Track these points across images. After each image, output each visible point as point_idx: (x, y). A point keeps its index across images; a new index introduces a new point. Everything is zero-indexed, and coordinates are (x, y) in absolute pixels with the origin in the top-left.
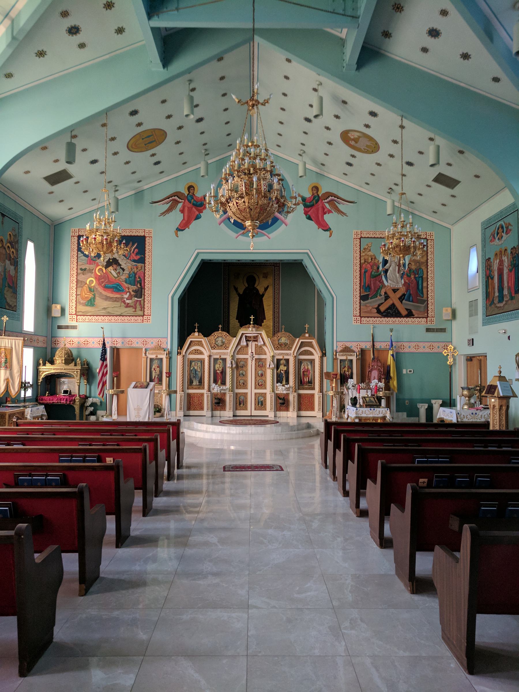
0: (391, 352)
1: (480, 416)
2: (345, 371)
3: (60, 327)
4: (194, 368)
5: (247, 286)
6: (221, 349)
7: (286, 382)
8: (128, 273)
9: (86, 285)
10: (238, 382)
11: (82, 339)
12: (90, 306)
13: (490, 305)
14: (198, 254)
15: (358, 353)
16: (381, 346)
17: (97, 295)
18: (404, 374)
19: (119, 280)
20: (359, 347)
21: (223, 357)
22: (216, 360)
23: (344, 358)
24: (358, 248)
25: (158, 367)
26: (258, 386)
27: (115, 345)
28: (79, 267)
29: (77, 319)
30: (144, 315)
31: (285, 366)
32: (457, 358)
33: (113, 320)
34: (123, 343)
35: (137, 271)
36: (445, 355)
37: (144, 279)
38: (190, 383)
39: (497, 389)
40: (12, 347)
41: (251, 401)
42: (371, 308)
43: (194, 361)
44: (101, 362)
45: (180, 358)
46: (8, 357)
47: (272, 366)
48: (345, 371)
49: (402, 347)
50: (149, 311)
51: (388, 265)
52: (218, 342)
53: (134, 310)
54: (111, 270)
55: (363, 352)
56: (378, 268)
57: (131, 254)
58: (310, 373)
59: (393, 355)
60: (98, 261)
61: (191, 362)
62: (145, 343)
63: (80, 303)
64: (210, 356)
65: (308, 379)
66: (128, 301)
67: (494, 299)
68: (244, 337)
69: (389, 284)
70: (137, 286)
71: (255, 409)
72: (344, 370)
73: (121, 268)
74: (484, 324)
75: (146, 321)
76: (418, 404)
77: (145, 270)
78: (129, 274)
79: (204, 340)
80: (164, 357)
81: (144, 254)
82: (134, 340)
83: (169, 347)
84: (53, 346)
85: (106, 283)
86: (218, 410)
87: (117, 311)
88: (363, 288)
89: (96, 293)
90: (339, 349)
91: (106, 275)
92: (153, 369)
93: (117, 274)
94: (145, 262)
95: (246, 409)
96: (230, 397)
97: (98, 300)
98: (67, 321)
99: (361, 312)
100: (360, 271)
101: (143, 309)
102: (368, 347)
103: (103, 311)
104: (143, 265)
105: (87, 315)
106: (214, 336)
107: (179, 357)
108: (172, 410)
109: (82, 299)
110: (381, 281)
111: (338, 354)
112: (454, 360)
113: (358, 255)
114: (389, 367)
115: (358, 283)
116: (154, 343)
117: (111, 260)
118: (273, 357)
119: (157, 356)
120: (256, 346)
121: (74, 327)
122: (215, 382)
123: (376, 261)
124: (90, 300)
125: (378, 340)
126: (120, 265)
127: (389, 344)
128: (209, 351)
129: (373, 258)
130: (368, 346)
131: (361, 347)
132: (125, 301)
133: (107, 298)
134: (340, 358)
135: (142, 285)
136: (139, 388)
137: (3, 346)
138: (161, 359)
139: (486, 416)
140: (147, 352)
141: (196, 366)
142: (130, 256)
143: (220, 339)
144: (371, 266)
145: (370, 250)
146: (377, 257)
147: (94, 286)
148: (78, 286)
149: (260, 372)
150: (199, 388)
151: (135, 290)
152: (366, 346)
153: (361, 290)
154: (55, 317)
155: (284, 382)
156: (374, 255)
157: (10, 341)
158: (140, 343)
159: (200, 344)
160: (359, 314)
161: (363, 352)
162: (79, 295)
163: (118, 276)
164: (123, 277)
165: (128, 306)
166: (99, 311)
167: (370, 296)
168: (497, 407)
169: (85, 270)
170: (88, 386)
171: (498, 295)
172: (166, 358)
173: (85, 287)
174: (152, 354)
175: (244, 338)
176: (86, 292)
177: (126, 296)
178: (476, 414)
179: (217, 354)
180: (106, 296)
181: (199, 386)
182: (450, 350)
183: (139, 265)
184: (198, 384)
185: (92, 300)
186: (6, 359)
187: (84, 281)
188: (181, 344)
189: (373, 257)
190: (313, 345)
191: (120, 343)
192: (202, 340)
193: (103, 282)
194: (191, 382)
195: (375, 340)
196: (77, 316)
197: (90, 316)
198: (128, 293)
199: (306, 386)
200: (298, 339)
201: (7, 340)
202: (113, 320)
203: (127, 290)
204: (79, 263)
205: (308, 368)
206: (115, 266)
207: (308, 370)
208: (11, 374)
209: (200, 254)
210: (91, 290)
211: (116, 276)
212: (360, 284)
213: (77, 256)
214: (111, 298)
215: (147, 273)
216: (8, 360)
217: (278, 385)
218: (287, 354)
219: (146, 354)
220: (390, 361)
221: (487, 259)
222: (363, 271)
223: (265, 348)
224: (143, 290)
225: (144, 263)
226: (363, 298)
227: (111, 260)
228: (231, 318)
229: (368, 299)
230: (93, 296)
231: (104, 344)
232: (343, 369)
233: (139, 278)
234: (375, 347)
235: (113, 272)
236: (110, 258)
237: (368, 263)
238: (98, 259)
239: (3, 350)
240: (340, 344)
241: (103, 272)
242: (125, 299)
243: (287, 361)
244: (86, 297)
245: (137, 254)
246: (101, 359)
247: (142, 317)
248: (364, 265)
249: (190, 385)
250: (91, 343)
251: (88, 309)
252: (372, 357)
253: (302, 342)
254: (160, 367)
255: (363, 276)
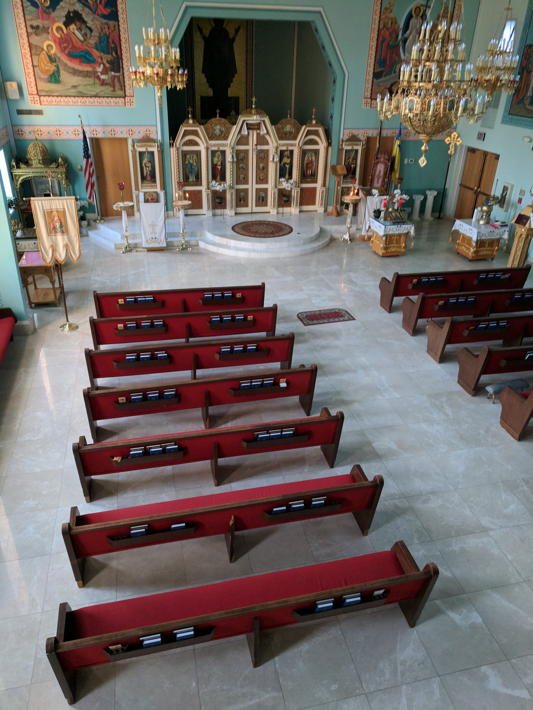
0: (398, 142)
1: (496, 233)
2: (349, 162)
3: (20, 112)
4: (189, 162)
5: (214, 25)
6: (219, 139)
7: (289, 176)
8: (98, 35)
9: (44, 52)
10: (238, 177)
11: (52, 128)
12: (55, 83)
13: (518, 103)
14: (187, 8)
15: (364, 143)
16: (387, 134)
17: (60, 67)
18: (406, 164)
19: (86, 45)
20: (365, 135)
21: (222, 148)
22: (214, 153)
23: (349, 148)
24: (379, 8)
25: (150, 162)
26: (259, 180)
27: (95, 136)
28: (29, 23)
29: (40, 102)
30: (125, 97)
31: (288, 158)
32: (459, 148)
33: (87, 102)
34: (104, 133)
35: (110, 33)
36: (448, 143)
37: (120, 45)
38: (186, 179)
39: (529, 220)
40: (64, 209)
41: (252, 198)
42: (383, 88)
43: (189, 154)
44: (85, 160)
45: (173, 151)
46: (63, 221)
47: (277, 159)
48: (349, 162)
49: (408, 135)
50: (132, 91)
51: (408, 32)
52: (216, 131)
53: (112, 89)
54: (74, 29)
55: (369, 139)
56: (397, 36)
57: (97, 6)
58: (313, 165)
59: (399, 146)
60: (53, 14)
61: (185, 154)
62: (131, 132)
63: (40, 78)
64: (207, 149)
65: (312, 171)
66: (103, 77)
67: (525, 98)
68: (245, 125)
69: (406, 58)
70: (112, 55)
71: (256, 206)
72: (348, 161)
73: (87, 27)
74: (504, 121)
75: (129, 104)
76: (413, 196)
77: (119, 31)
78: (100, 37)
79: (199, 129)
80: (155, 150)
81: (116, 6)
82: (117, 129)
83: (160, 138)
84: (16, 137)
85: (70, 49)
86: (218, 208)
87: (91, 91)
88: (377, 63)
89: (59, 64)
90: (346, 138)
91: (69, 38)
92: (143, 165)
93: (83, 36)
94: (118, 18)
95: (246, 205)
96: (232, 194)
97: (64, 75)
98: (28, 104)
99: (373, 93)
100: (377, 40)
101: (123, 88)
102: (375, 135)
103: (73, 90)
104: (116, 23)
105: (53, 96)
106: (211, 123)
107: (172, 149)
108: (169, 209)
109: (42, 72)
110: (398, 53)
111: (344, 143)
112: (456, 149)
113: (377, 17)
114: (394, 159)
115: (373, 57)
116: (142, 132)
117: (72, 15)
118: (277, 148)
119: (147, 149)
120: (258, 135)
121: (39, 112)
122: (214, 177)
123: (396, 27)
124: (53, 74)
125: (386, 127)
126: (85, 22)
127: (397, 132)
128: (207, 142)
129: (394, 22)
130: (373, 133)
131: (367, 135)
132: (99, 76)
133: (75, 72)
134: (346, 147)
135: (119, 53)
136: (151, 202)
137: (53, 208)
138: (152, 153)
139: (501, 233)
140: (135, 144)
141: (192, 160)
142: (97, 9)
143: (218, 127)
144: (390, 34)
145: (391, 11)
146: (398, 20)
147: (55, 54)
148: (33, 52)
149: (261, 165)
150: (196, 185)
151: (111, 61)
152: (373, 134)
153: (376, 66)
154: (14, 100)
155: (287, 177)
156: (395, 18)
157: (60, 201)
158: (124, 133)
159: (195, 133)
160: (369, 96)
161: (369, 139)
162: (36, 66)
163: (85, 40)
164: (92, 41)
165: (103, 83)
166: (67, 89)
167: (384, 73)
168: (524, 236)
169: (37, 27)
170: (71, 186)
171: (531, 94)
172: (158, 151)
173: (43, 56)
174: (141, 146)
175: (245, 126)
176: (45, 62)
177: (100, 69)
178: (493, 231)
179: (214, 145)
180: (73, 68)
181: (196, 183)
182: (454, 138)
183: (112, 23)
184: (194, 180)
185: (56, 74)
186: (61, 222)
187: (39, 45)
188: (173, 134)
189: (394, 22)
190: (319, 134)
191: (101, 133)
192: (198, 129)
193: (65, 48)
194: (186, 178)
195: (383, 127)
196: (40, 96)
197: (57, 96)
198: (102, 66)
199: (309, 180)
200: (304, 127)
201: (57, 201)
202: (87, 102)
203: (100, 60)
204: (27, 17)
205: (312, 159)
206: (78, 23)
207: (312, 162)
208: (70, 239)
209: (189, 10)
210: (52, 59)
211: (82, 38)
212: (375, 57)
213: (22, 6)
214: (81, 72)
215: (123, 36)
216: (63, 224)
217: (281, 180)
218: (292, 145)
219: (133, 146)
220: (396, 151)
221: (527, 45)
222: (380, 39)
223: (267, 137)
224: (121, 61)
225: (117, 20)
226: (377, 75)
227: (72, 15)
228: (196, 71)
229: (381, 77)
230: (56, 69)
231: (85, 137)
232: (348, 160)
233: (113, 42)
234: (382, 135)
235: (77, 32)
236: (69, 10)
237: (387, 29)
238: (54, 11)
239: (56, 213)
240: (347, 132)
241: (63, 32)
242: (99, 74)
243: (292, 152)
244: (47, 71)
245: (106, 6)
246: (84, 156)
247: (122, 99)
248: (382, 32)
249: (186, 182)
250: (65, 133)
251: (53, 86)
252: (378, 145)
253: (308, 131)
254: (152, 161)
255: (380, 47)
